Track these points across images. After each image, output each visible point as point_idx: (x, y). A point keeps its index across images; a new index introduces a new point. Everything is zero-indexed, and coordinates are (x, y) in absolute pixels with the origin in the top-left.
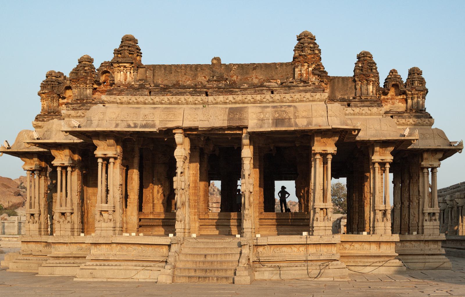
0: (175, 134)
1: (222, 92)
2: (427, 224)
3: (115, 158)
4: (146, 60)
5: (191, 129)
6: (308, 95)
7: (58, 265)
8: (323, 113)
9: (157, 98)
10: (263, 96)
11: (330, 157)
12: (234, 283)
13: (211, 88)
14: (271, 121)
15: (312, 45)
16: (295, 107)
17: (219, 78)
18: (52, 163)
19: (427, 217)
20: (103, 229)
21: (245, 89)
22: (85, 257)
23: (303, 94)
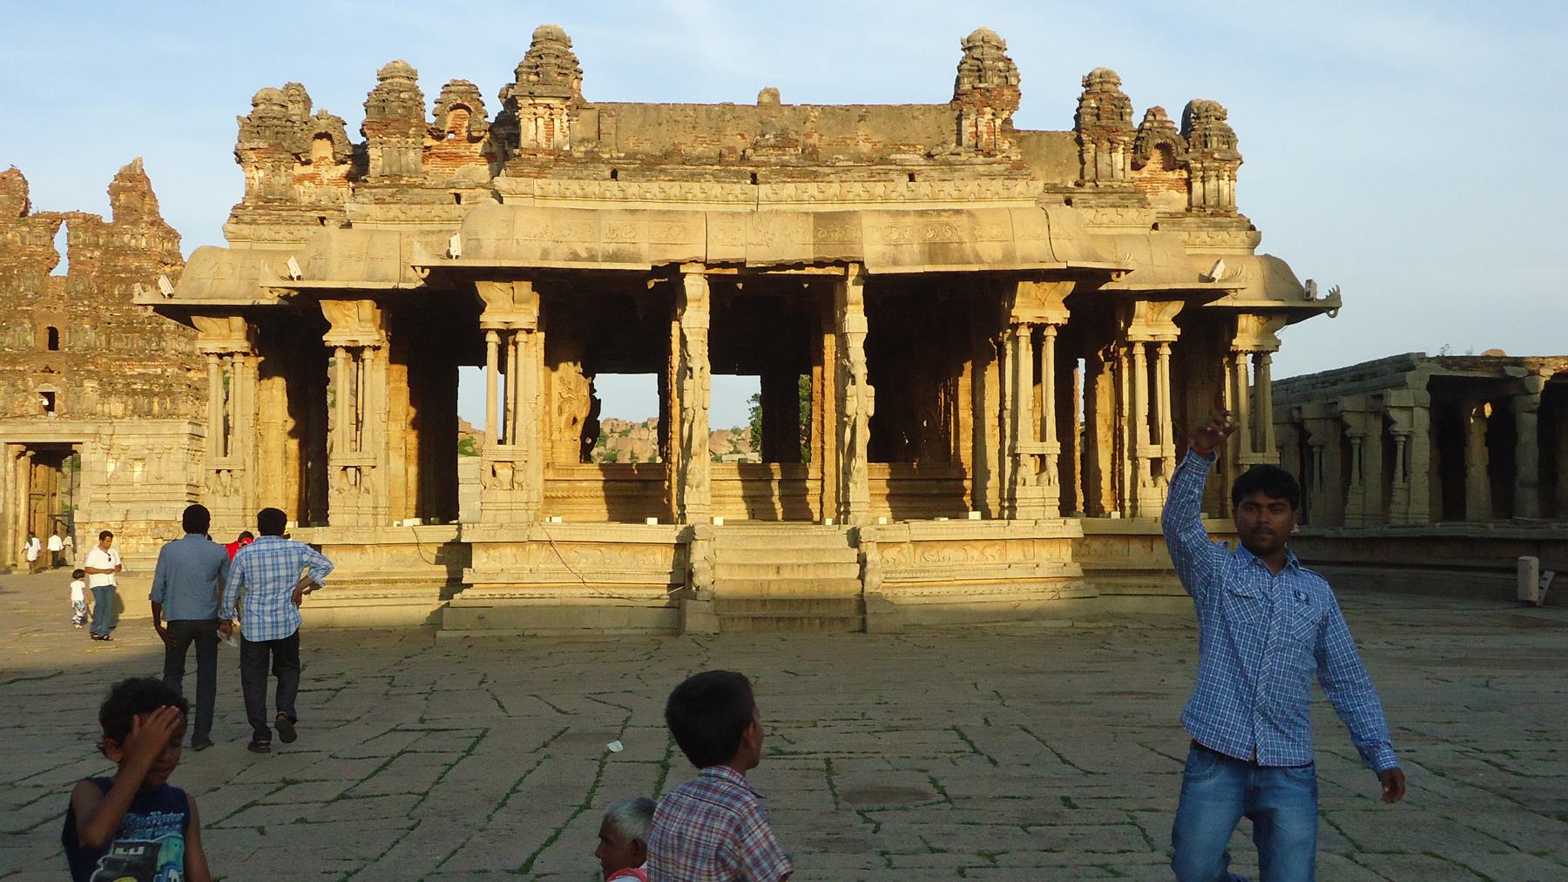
0: (684, 275)
1: (791, 176)
4: (593, 90)
6: (997, 185)
10: (891, 186)
11: (1051, 333)
12: (863, 630)
13: (765, 164)
14: (916, 248)
15: (1001, 65)
16: (970, 213)
17: (775, 141)
21: (847, 170)
23: (985, 182)
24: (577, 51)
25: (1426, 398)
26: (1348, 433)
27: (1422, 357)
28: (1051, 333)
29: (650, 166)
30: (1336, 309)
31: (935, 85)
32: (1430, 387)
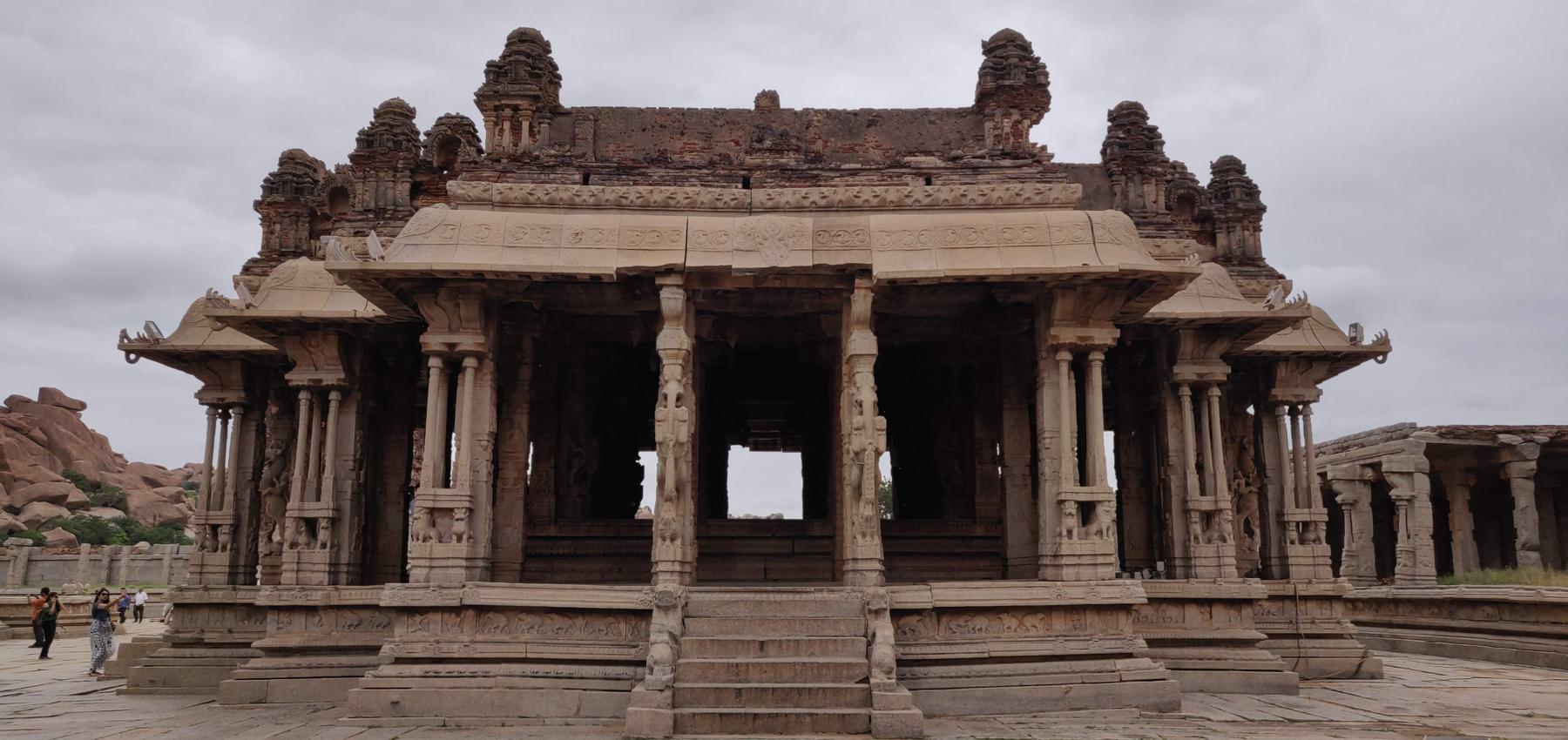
0: (661, 286)
1: (789, 179)
2: (1295, 551)
3: (479, 357)
4: (569, 97)
5: (707, 276)
6: (1029, 189)
7: (284, 673)
8: (1080, 233)
9: (608, 189)
11: (1097, 358)
13: (759, 167)
18: (287, 377)
19: (1294, 535)
20: (434, 563)
21: (854, 172)
22: (375, 650)
24: (556, 55)
25: (1425, 463)
26: (1339, 499)
27: (1413, 427)
28: (1097, 358)
29: (626, 171)
30: (1385, 354)
31: (954, 84)
32: (1427, 454)
